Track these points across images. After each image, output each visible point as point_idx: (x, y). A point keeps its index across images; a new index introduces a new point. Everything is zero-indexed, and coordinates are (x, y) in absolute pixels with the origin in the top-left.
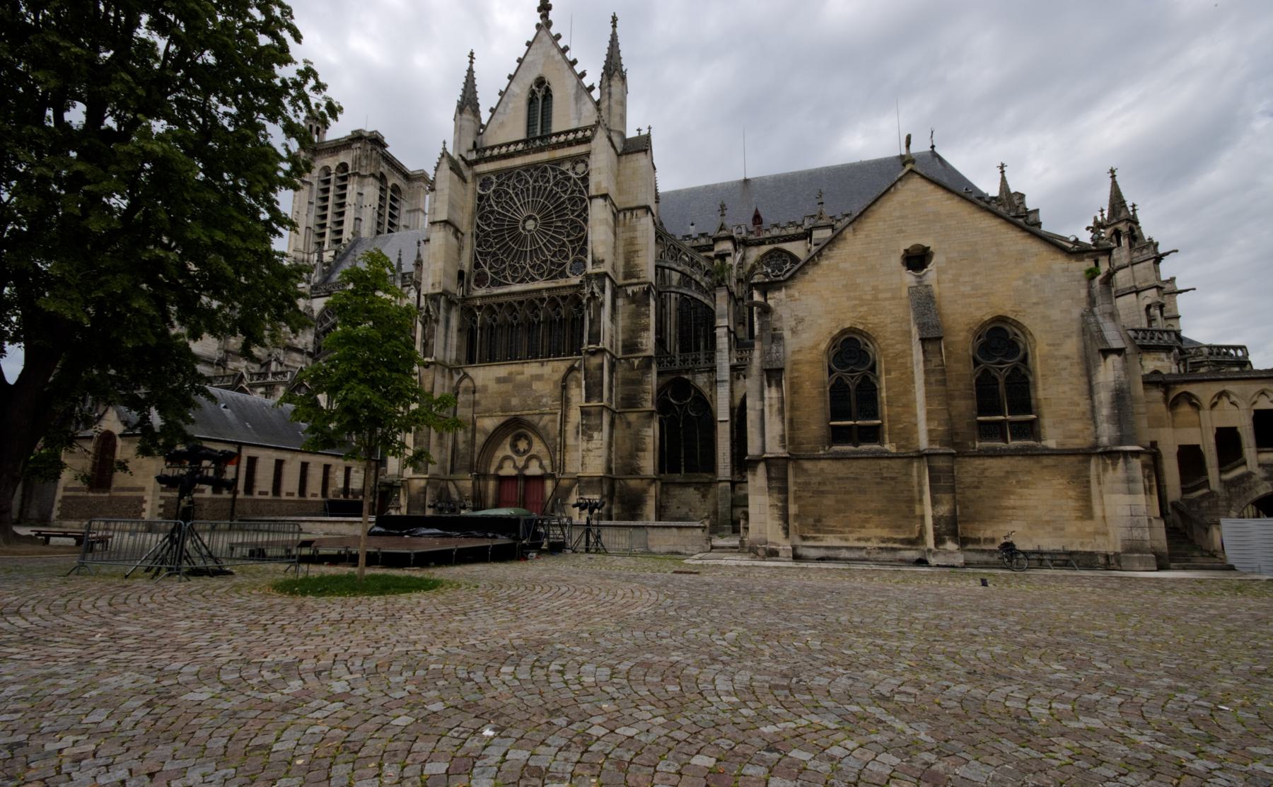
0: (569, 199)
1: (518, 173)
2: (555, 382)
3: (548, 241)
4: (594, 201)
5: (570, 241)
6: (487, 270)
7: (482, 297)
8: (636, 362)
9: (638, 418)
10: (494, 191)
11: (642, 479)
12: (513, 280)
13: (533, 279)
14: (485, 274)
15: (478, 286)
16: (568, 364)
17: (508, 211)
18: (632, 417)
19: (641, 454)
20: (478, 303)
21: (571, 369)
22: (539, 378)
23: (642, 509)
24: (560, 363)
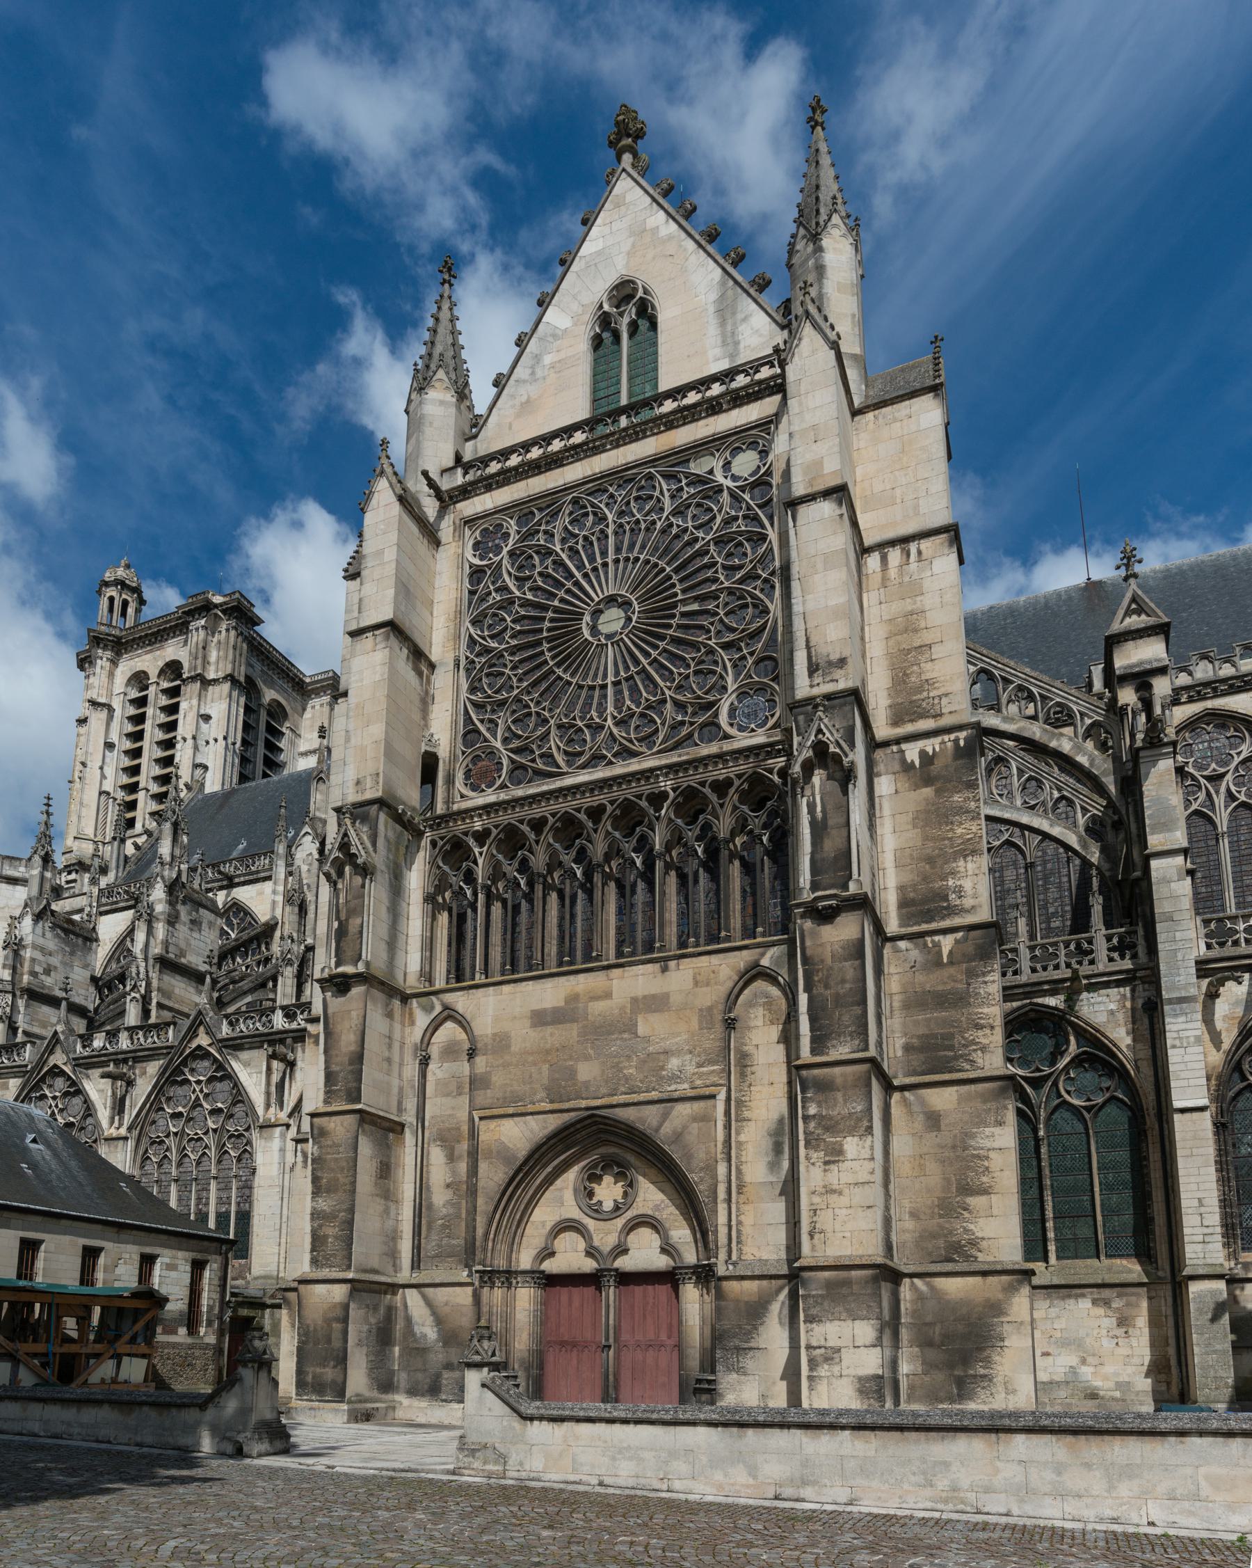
0: (718, 541)
1: (575, 501)
2: (706, 1014)
6: (498, 744)
7: (488, 809)
8: (947, 943)
9: (961, 1099)
11: (984, 1274)
12: (569, 764)
14: (492, 753)
15: (475, 788)
16: (742, 959)
18: (943, 1099)
19: (974, 1201)
20: (478, 825)
21: (754, 973)
22: (656, 1003)
23: (988, 1362)
24: (715, 960)
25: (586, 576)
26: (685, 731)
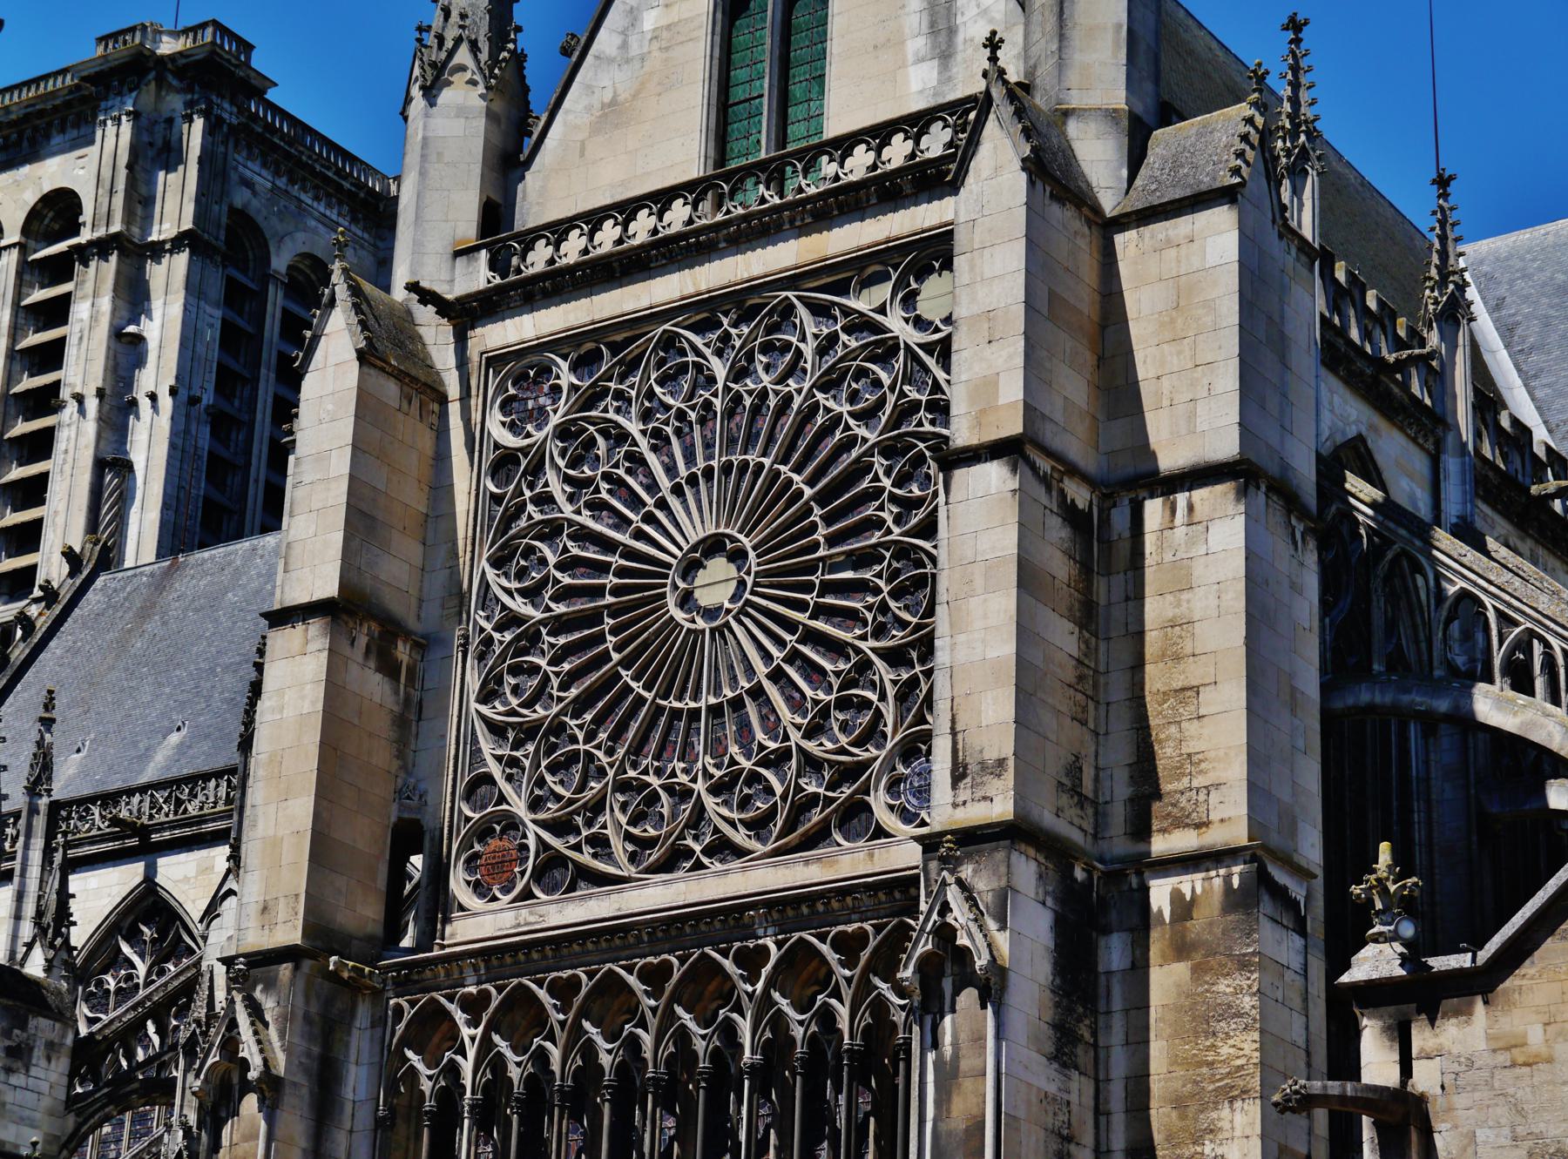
3: (794, 657)
4: (959, 474)
5: (884, 654)
10: (563, 433)
13: (723, 849)
17: (622, 522)
25: (640, 535)
26: (816, 816)
